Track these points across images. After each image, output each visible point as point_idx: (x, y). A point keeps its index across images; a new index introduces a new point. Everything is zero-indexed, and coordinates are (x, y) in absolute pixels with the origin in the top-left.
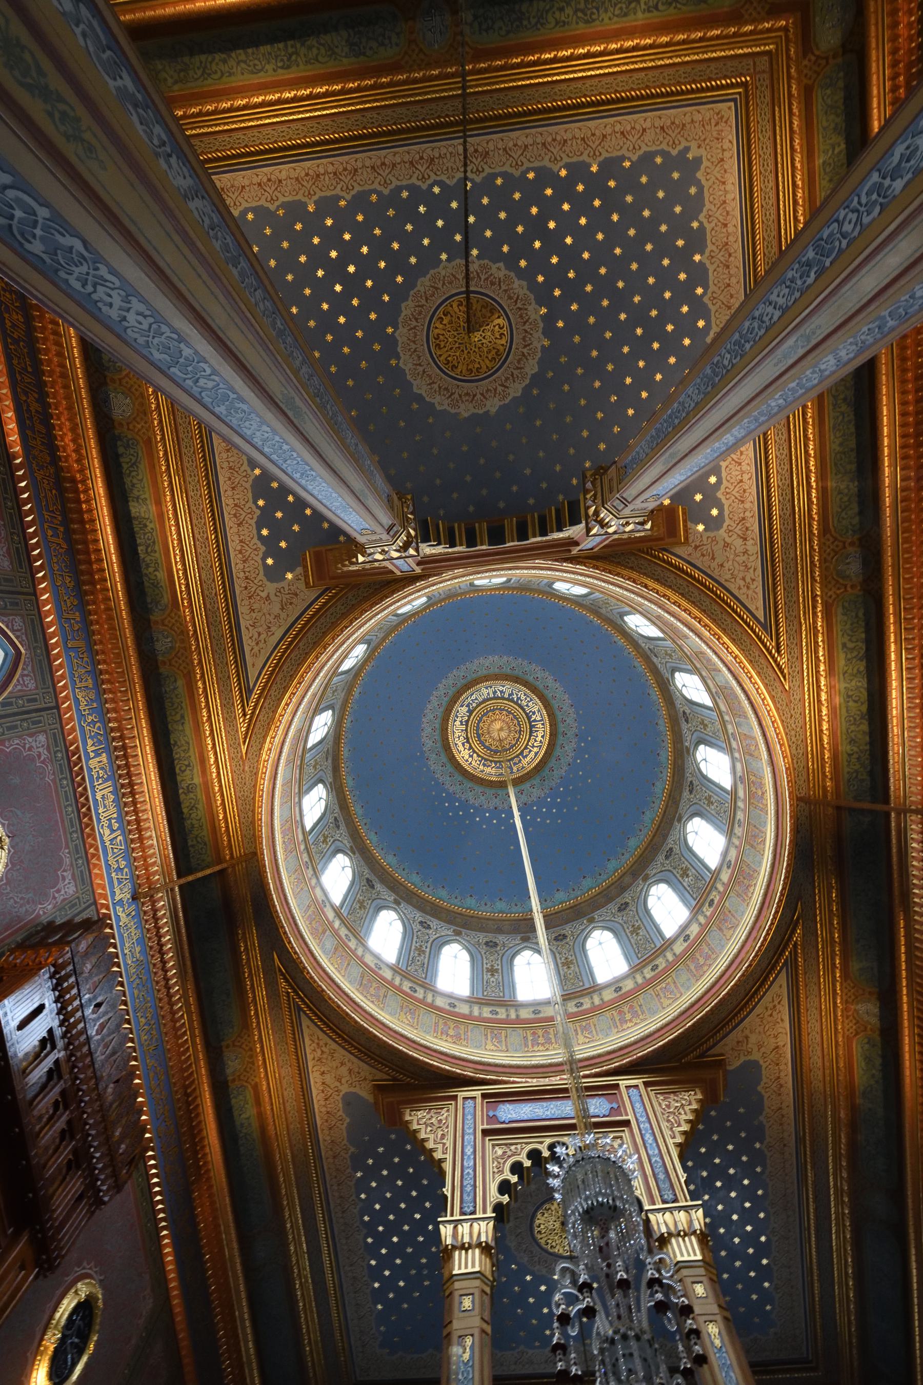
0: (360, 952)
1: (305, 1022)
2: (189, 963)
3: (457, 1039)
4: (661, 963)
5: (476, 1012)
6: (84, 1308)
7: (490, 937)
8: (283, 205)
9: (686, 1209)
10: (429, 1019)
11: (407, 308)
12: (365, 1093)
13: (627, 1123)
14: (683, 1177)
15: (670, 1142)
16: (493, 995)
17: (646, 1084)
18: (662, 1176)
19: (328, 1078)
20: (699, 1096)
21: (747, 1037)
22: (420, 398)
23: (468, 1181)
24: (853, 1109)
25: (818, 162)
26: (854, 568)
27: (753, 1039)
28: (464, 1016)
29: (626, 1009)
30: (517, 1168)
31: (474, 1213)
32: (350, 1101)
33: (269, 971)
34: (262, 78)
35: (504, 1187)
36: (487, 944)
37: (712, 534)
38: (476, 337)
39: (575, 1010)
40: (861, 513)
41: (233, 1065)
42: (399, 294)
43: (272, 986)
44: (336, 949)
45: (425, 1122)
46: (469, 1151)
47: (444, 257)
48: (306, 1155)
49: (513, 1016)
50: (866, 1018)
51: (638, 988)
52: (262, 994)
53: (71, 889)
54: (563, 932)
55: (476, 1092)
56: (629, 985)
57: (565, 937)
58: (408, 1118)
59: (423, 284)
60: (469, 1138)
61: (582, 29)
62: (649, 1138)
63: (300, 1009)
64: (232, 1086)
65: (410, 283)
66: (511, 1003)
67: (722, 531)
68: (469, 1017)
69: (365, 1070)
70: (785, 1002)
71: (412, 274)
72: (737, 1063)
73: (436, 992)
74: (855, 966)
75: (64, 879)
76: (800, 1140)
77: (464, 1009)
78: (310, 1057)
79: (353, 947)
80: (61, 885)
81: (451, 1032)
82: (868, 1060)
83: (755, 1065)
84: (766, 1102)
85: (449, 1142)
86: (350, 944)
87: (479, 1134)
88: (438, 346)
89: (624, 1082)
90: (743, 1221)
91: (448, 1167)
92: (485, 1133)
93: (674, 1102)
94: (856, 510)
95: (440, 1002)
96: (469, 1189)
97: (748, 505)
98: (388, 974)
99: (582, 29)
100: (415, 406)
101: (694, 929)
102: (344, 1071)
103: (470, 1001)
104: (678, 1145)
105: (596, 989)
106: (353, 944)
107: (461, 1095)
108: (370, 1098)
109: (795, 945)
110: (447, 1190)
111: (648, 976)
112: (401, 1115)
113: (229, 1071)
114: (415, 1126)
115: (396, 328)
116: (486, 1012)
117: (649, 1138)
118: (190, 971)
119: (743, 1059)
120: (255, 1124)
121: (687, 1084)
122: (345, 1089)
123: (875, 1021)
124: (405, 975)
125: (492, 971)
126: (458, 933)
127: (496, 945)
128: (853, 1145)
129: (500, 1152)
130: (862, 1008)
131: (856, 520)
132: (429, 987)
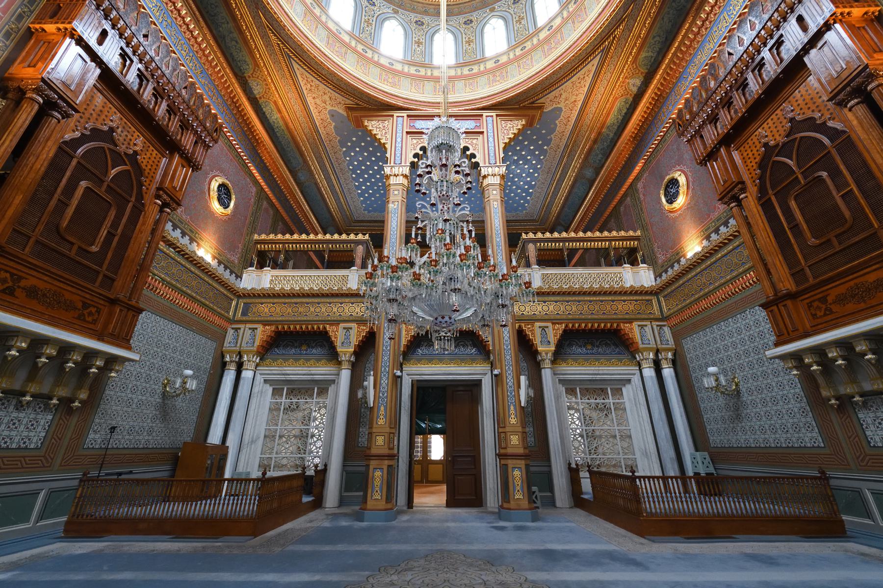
0: (324, 18)
1: (296, 66)
2: (197, 13)
3: (394, 85)
4: (528, 45)
5: (406, 70)
7: (419, 17)
9: (498, 167)
10: (376, 71)
12: (341, 111)
13: (482, 133)
14: (502, 155)
15: (501, 142)
16: (419, 59)
17: (497, 116)
19: (318, 101)
20: (524, 123)
21: (561, 95)
24: (599, 134)
27: (563, 96)
28: (398, 72)
29: (498, 74)
32: (333, 114)
33: (260, 26)
36: (416, 22)
39: (468, 73)
41: (257, 90)
43: (264, 36)
44: (306, 14)
45: (375, 126)
46: (399, 140)
48: (314, 139)
49: (429, 74)
50: (631, 87)
51: (510, 62)
52: (260, 43)
54: (471, 18)
55: (404, 114)
56: (504, 59)
57: (471, 21)
58: (366, 124)
60: (400, 135)
62: (491, 139)
63: (290, 57)
66: (429, 66)
68: (401, 73)
69: (340, 98)
70: (591, 76)
72: (550, 109)
73: (380, 54)
74: (643, 54)
76: (567, 146)
77: (398, 67)
78: (304, 88)
79: (318, 14)
81: (390, 80)
82: (620, 110)
83: (560, 110)
84: (558, 129)
85: (389, 136)
86: (315, 11)
87: (405, 133)
89: (485, 113)
90: (527, 176)
91: (388, 146)
92: (408, 133)
93: (509, 124)
95: (383, 61)
98: (346, 38)
101: (558, 21)
102: (326, 97)
103: (404, 62)
104: (506, 143)
105: (483, 60)
106: (317, 11)
107: (395, 115)
108: (345, 114)
109: (614, 38)
110: (388, 155)
111: (517, 54)
112: (363, 123)
113: (255, 92)
114: (370, 128)
116: (413, 70)
117: (491, 139)
118: (201, 19)
119: (555, 106)
120: (281, 123)
121: (518, 116)
122: (329, 108)
123: (635, 90)
124: (359, 40)
125: (419, 43)
126: (396, 12)
127: (423, 24)
128: (591, 150)
129: (415, 141)
130: (632, 81)
132: (375, 51)
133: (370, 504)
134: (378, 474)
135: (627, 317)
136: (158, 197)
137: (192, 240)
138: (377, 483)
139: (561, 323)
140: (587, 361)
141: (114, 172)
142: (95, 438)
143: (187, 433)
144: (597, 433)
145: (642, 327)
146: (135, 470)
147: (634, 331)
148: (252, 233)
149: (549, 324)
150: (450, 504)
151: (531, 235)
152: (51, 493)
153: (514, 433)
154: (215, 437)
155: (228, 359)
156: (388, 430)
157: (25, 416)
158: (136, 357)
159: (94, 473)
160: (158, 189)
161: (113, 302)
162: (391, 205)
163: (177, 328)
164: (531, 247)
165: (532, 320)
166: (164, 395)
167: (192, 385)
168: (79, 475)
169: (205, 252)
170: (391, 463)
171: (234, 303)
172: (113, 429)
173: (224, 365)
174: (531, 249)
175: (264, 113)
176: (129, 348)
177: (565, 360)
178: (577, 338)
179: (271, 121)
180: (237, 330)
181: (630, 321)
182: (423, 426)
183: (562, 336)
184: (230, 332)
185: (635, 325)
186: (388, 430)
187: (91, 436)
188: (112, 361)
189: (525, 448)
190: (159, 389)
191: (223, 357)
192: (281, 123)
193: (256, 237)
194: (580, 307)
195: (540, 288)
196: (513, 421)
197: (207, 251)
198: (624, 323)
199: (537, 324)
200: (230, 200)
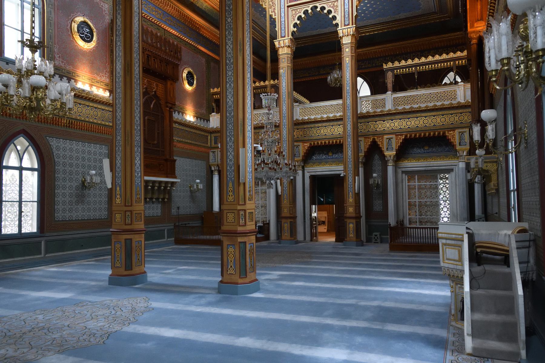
6: (189, 73)
18: (347, 16)
23: (283, 26)
30: (300, 18)
31: (285, 37)
35: (295, 25)
53: (107, 6)
64: (194, 2)
75: (102, 6)
80: (104, 9)
92: (288, 7)
96: (283, 28)
110: (277, 29)
133: (283, 237)
134: (286, 225)
135: (451, 126)
136: (167, 107)
137: (183, 113)
138: (286, 228)
139: (402, 135)
140: (418, 159)
141: (152, 106)
142: (174, 211)
143: (204, 207)
144: (428, 203)
145: (463, 133)
146: (190, 223)
147: (455, 137)
148: (209, 90)
149: (394, 136)
150: (336, 241)
151: (390, 65)
152: (168, 230)
153: (351, 206)
154: (216, 207)
155: (213, 169)
156: (289, 206)
157: (155, 205)
158: (179, 180)
159: (177, 224)
160: (167, 103)
161: (166, 160)
162: (281, 71)
163: (188, 160)
164: (390, 75)
165: (382, 134)
166: (191, 191)
167: (201, 186)
168: (173, 224)
169: (190, 117)
170: (292, 220)
171: (209, 137)
172: (178, 208)
173: (212, 173)
174: (390, 79)
175: (198, 7)
176: (175, 178)
177: (406, 158)
178: (410, 144)
179: (203, 9)
180: (214, 152)
181: (453, 129)
182: (322, 200)
183: (402, 143)
184: (211, 154)
185: (457, 131)
186: (289, 206)
187: (173, 211)
188: (173, 183)
189: (356, 214)
190: (188, 189)
191: (211, 168)
192: (209, 7)
193: (212, 91)
194: (417, 122)
195: (390, 110)
196: (351, 200)
197: (190, 115)
198: (448, 131)
199: (386, 137)
200: (193, 79)
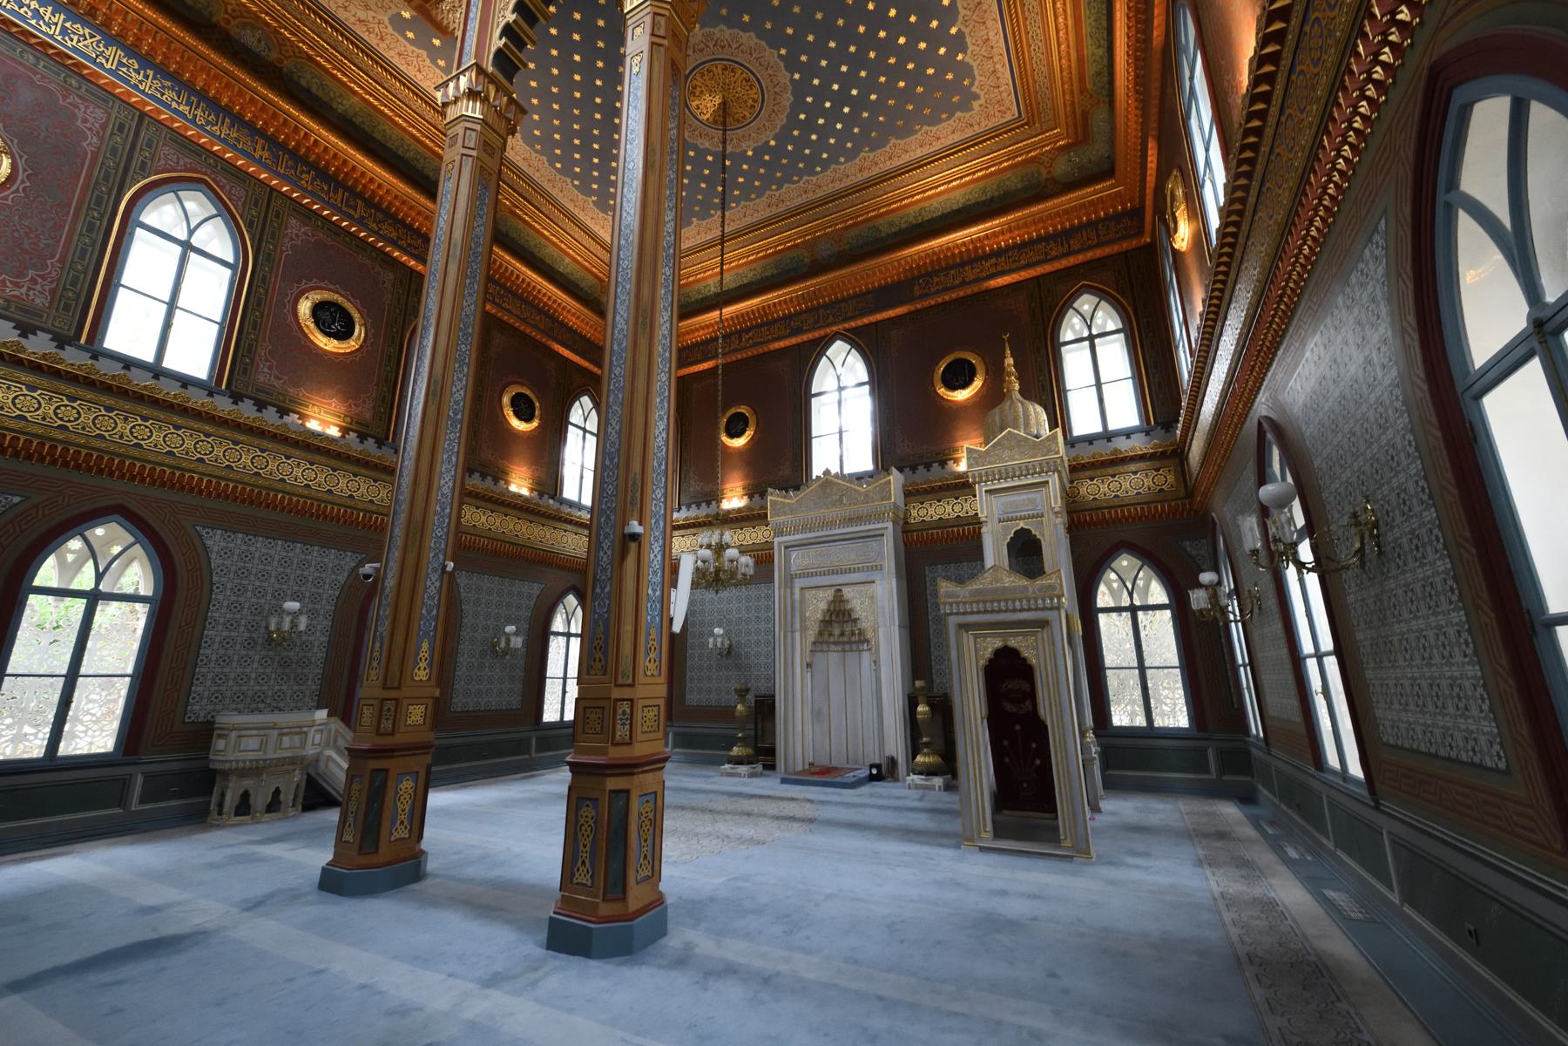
8: (916, 132)
11: (788, 98)
22: (745, 28)
25: (567, 260)
26: (249, 39)
34: (940, 199)
37: (390, 13)
38: (718, 100)
40: (308, 91)
42: (798, 105)
47: (773, 143)
59: (781, 120)
61: (740, 271)
65: (793, 116)
67: (386, 19)
71: (793, 122)
88: (748, 80)
94: (314, 90)
97: (392, 53)
99: (740, 271)
100: (746, 18)
115: (792, 80)
131: (303, 83)
